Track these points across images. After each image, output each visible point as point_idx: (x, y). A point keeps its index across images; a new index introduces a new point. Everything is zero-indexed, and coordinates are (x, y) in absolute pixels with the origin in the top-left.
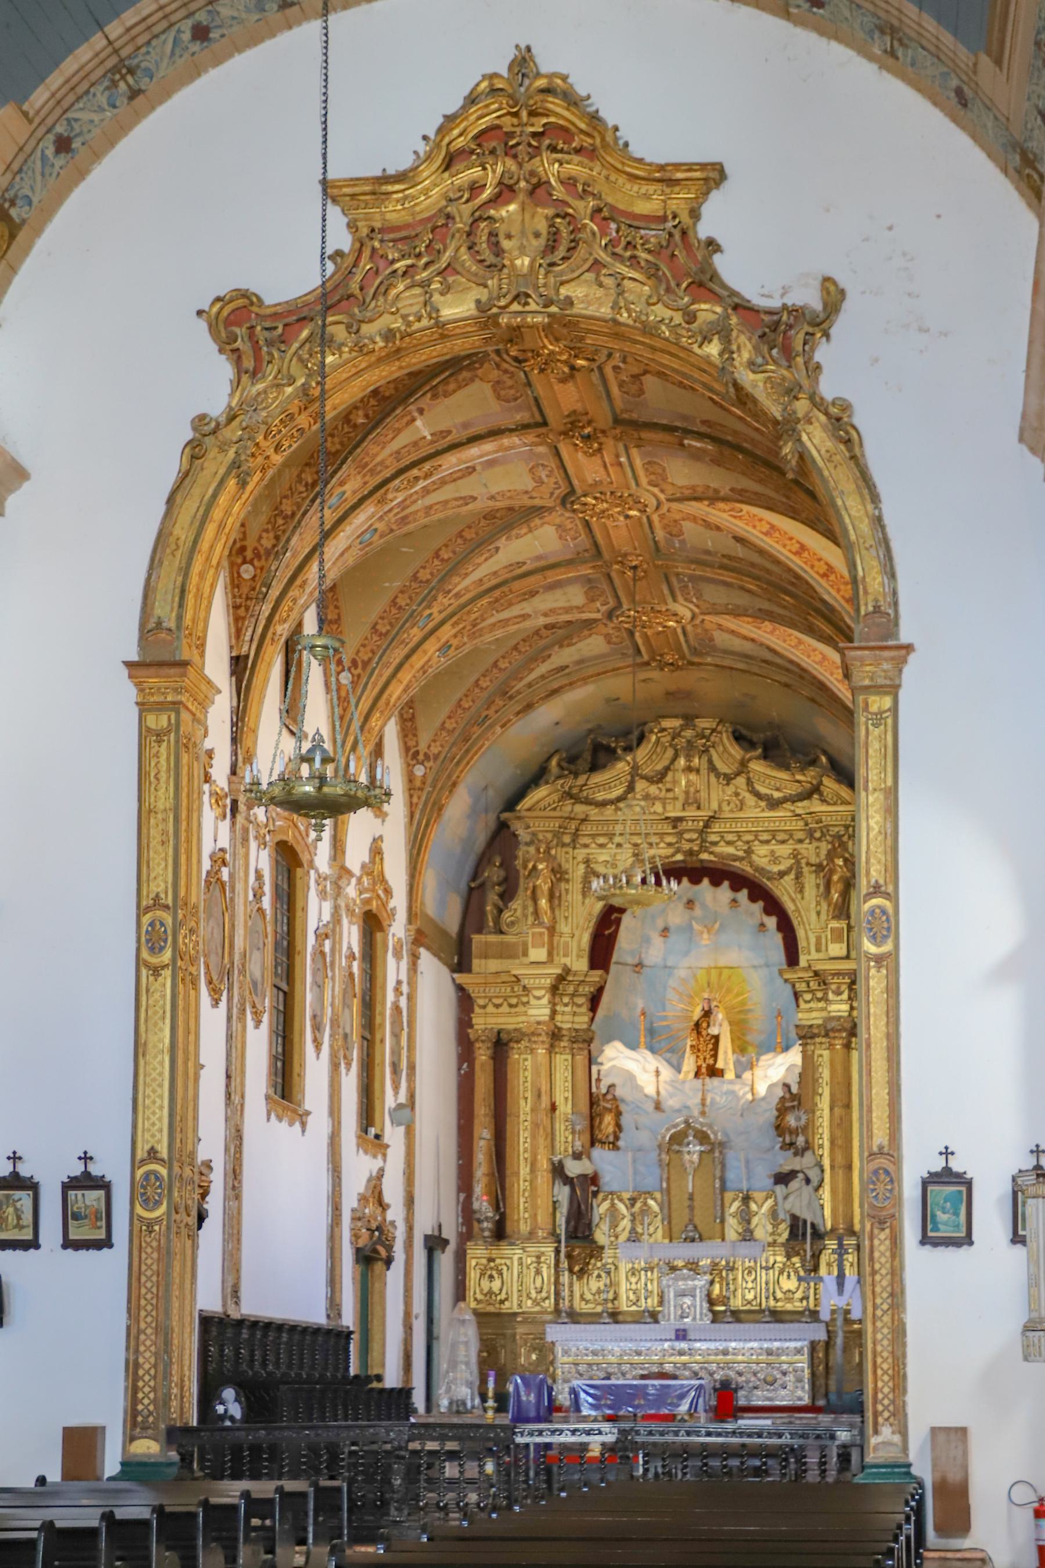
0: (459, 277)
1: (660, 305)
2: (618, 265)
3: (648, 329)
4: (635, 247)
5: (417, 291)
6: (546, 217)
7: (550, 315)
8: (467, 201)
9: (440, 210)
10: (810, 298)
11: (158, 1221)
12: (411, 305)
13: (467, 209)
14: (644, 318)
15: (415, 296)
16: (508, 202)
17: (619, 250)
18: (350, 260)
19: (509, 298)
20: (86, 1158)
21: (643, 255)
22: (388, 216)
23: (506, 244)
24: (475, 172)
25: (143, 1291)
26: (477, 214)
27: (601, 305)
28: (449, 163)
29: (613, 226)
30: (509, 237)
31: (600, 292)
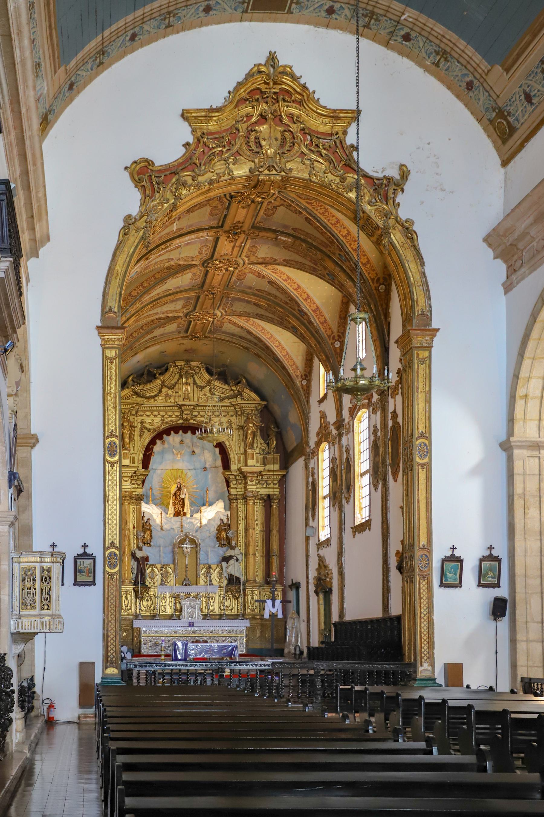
3: (323, 186)
7: (282, 176)
8: (244, 122)
9: (233, 125)
11: (115, 574)
13: (245, 126)
14: (323, 179)
19: (265, 167)
20: (85, 546)
22: (210, 127)
23: (263, 143)
24: (249, 109)
25: (110, 604)
26: (250, 128)
27: (304, 172)
28: (236, 106)
30: (264, 139)
31: (303, 167)
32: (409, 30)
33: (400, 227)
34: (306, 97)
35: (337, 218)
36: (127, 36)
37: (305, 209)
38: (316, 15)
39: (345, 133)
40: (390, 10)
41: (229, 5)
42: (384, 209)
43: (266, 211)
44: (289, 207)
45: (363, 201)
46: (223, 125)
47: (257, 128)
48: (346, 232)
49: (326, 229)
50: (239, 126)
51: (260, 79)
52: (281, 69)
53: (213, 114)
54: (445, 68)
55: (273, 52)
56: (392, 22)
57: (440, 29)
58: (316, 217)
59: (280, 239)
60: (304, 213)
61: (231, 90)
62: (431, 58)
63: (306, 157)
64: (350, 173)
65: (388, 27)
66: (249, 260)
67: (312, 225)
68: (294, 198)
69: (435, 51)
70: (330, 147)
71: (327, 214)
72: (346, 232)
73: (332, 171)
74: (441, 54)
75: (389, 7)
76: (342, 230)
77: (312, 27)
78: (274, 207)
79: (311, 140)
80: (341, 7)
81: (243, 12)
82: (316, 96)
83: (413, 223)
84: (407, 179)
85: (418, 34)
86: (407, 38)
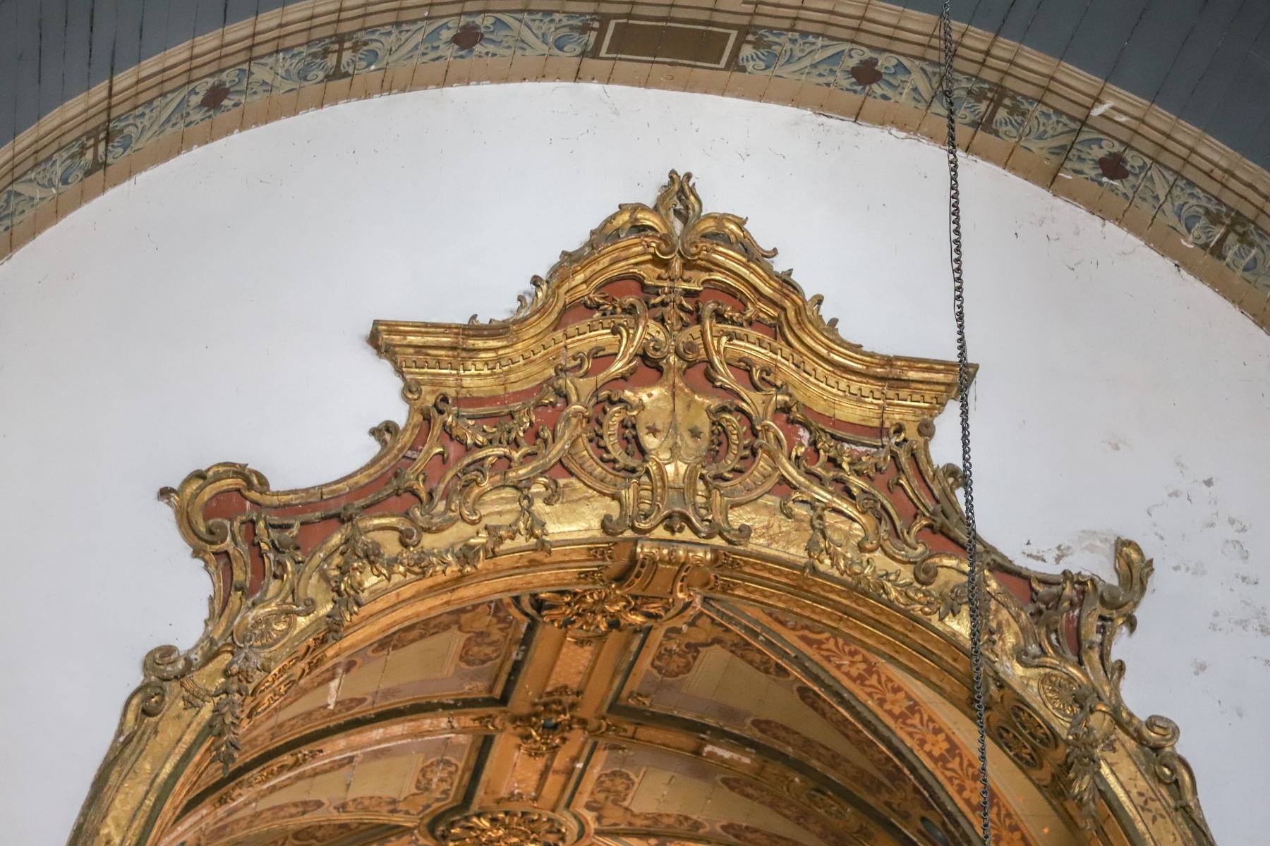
0: (573, 480)
1: (878, 554)
2: (816, 488)
3: (857, 589)
4: (840, 467)
5: (509, 493)
6: (708, 410)
7: (715, 550)
8: (586, 375)
9: (548, 381)
10: (1105, 572)
12: (500, 513)
13: (587, 385)
14: (857, 569)
15: (507, 501)
16: (651, 384)
17: (819, 470)
18: (406, 439)
21: (857, 483)
22: (467, 382)
23: (650, 442)
26: (604, 393)
29: (804, 435)
30: (653, 431)
31: (787, 525)
32: (1118, 148)
33: (1131, 744)
34: (791, 314)
35: (909, 697)
36: (194, 92)
37: (798, 660)
38: (822, 80)
39: (926, 430)
40: (1055, 86)
41: (539, 33)
42: (1071, 678)
43: (659, 657)
44: (741, 648)
45: (997, 648)
46: (513, 377)
47: (628, 393)
48: (945, 745)
49: (875, 732)
50: (567, 383)
51: (640, 248)
52: (709, 226)
53: (480, 344)
54: (1243, 263)
55: (681, 173)
56: (1064, 119)
57: (1215, 151)
58: (837, 687)
59: (711, 754)
60: (796, 672)
61: (543, 274)
62: (1196, 231)
63: (796, 495)
64: (950, 557)
65: (1051, 132)
66: (599, 819)
67: (824, 714)
68: (757, 622)
69: (1208, 212)
70: (878, 470)
71: (874, 680)
72: (945, 745)
73: (887, 545)
74: (1228, 221)
75: (1052, 78)
76: (930, 737)
77: (808, 113)
78: (688, 646)
79: (814, 443)
80: (900, 64)
81: (583, 54)
82: (827, 313)
83: (1176, 732)
84: (1143, 589)
85: (1149, 161)
86: (1113, 167)
